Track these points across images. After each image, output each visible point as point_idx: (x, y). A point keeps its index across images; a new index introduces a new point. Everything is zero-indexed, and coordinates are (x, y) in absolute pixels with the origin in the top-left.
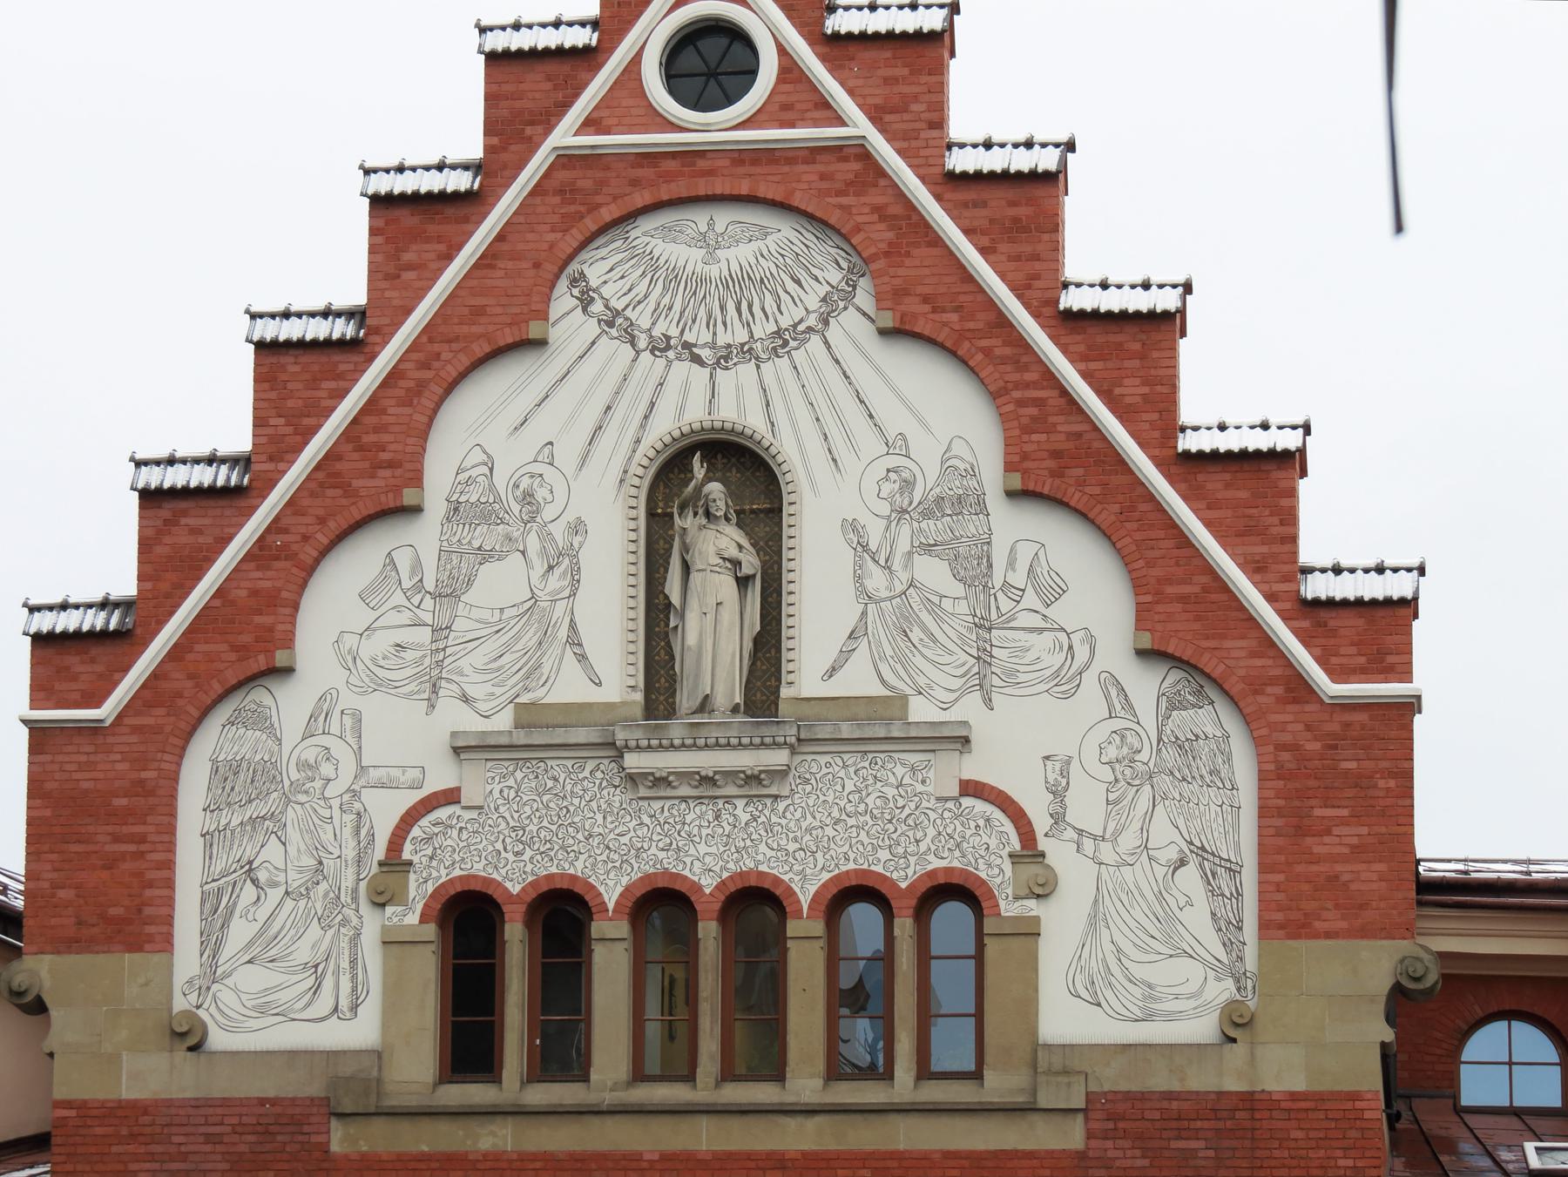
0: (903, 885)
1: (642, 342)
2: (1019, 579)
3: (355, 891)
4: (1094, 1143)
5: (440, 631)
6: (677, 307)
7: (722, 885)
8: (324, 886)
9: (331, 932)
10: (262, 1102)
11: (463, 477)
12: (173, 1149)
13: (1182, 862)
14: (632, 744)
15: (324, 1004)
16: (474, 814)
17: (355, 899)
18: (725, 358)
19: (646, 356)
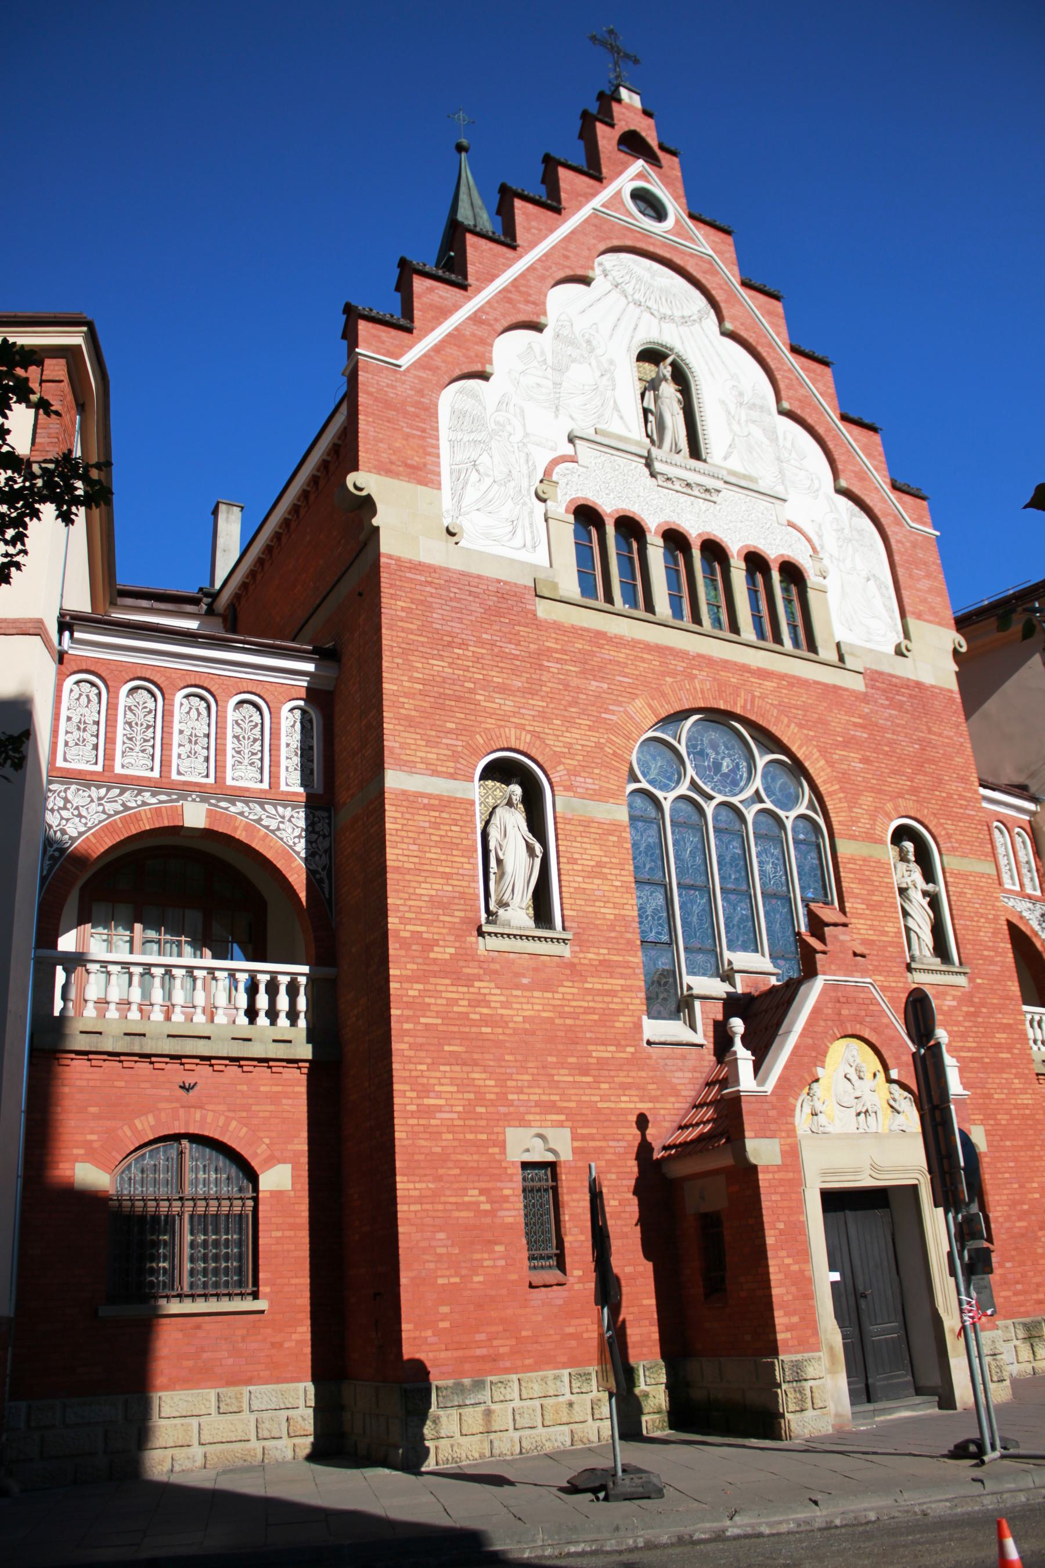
0: (772, 557)
1: (630, 299)
2: (788, 445)
3: (529, 490)
4: (870, 690)
5: (557, 385)
6: (642, 291)
7: (699, 535)
8: (512, 484)
9: (518, 507)
10: (499, 581)
11: (560, 323)
12: (452, 595)
13: (868, 580)
14: (659, 458)
15: (518, 542)
16: (584, 470)
17: (529, 494)
18: (663, 318)
19: (632, 305)
